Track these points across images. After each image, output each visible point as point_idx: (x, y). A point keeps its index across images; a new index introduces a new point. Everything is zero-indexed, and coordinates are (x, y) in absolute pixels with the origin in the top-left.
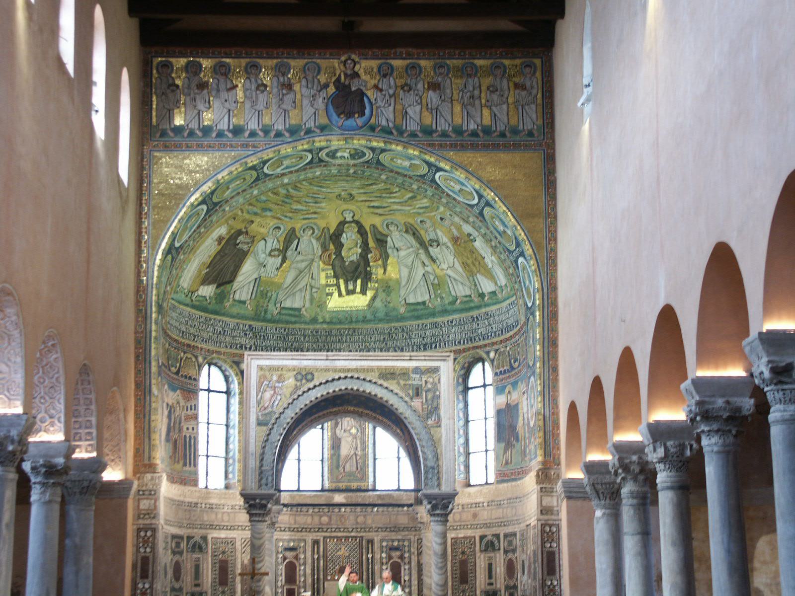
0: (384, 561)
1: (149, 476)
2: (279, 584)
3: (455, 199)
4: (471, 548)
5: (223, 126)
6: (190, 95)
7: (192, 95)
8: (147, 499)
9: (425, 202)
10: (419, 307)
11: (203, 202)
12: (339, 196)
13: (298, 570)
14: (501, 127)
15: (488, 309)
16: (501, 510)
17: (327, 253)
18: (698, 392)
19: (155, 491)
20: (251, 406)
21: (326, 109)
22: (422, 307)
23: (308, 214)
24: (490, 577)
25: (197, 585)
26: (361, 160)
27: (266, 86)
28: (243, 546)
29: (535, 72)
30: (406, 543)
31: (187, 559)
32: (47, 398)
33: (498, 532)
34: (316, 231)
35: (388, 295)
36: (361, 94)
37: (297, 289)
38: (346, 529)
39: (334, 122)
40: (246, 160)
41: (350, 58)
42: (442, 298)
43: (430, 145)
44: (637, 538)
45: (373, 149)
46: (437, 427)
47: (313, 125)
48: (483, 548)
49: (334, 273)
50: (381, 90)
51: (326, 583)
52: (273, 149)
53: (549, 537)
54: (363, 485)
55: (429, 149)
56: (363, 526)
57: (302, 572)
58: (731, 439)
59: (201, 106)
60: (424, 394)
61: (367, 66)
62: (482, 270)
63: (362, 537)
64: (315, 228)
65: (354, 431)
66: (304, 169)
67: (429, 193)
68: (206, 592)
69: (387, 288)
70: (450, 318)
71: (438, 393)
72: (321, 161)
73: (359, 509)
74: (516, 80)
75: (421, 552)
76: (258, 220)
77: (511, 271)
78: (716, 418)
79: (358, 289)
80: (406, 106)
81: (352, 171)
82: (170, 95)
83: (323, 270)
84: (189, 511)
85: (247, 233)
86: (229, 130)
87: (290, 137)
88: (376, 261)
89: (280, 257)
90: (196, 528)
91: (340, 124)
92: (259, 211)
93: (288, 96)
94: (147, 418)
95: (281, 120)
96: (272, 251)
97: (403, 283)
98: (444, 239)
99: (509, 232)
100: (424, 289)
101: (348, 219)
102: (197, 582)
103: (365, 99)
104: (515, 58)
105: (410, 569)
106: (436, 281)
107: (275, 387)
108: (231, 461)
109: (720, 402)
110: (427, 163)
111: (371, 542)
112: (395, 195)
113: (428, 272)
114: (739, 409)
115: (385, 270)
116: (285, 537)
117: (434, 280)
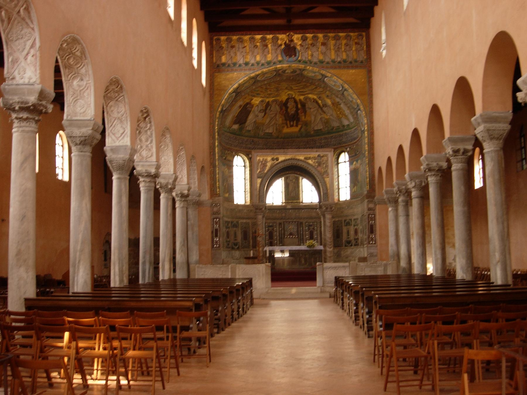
0: (307, 230)
1: (217, 198)
2: (267, 240)
5: (241, 62)
6: (227, 50)
9: (321, 90)
12: (286, 88)
14: (350, 60)
15: (347, 131)
18: (427, 160)
24: (348, 235)
25: (236, 240)
26: (296, 74)
29: (363, 39)
30: (315, 223)
32: (180, 168)
33: (350, 218)
36: (294, 48)
43: (323, 67)
44: (405, 217)
45: (300, 70)
48: (345, 224)
50: (303, 46)
51: (285, 240)
53: (371, 219)
54: (298, 201)
58: (438, 178)
59: (232, 54)
61: (297, 38)
62: (344, 116)
63: (298, 222)
65: (294, 180)
66: (272, 78)
69: (306, 124)
70: (332, 135)
72: (279, 74)
73: (297, 211)
74: (356, 41)
76: (255, 99)
77: (355, 116)
78: (434, 170)
79: (295, 125)
81: (291, 78)
83: (281, 117)
87: (267, 65)
88: (302, 113)
89: (263, 114)
91: (287, 60)
92: (255, 95)
96: (260, 110)
97: (313, 122)
101: (290, 97)
103: (297, 50)
104: (355, 32)
108: (246, 193)
109: (435, 164)
111: (302, 223)
114: (441, 167)
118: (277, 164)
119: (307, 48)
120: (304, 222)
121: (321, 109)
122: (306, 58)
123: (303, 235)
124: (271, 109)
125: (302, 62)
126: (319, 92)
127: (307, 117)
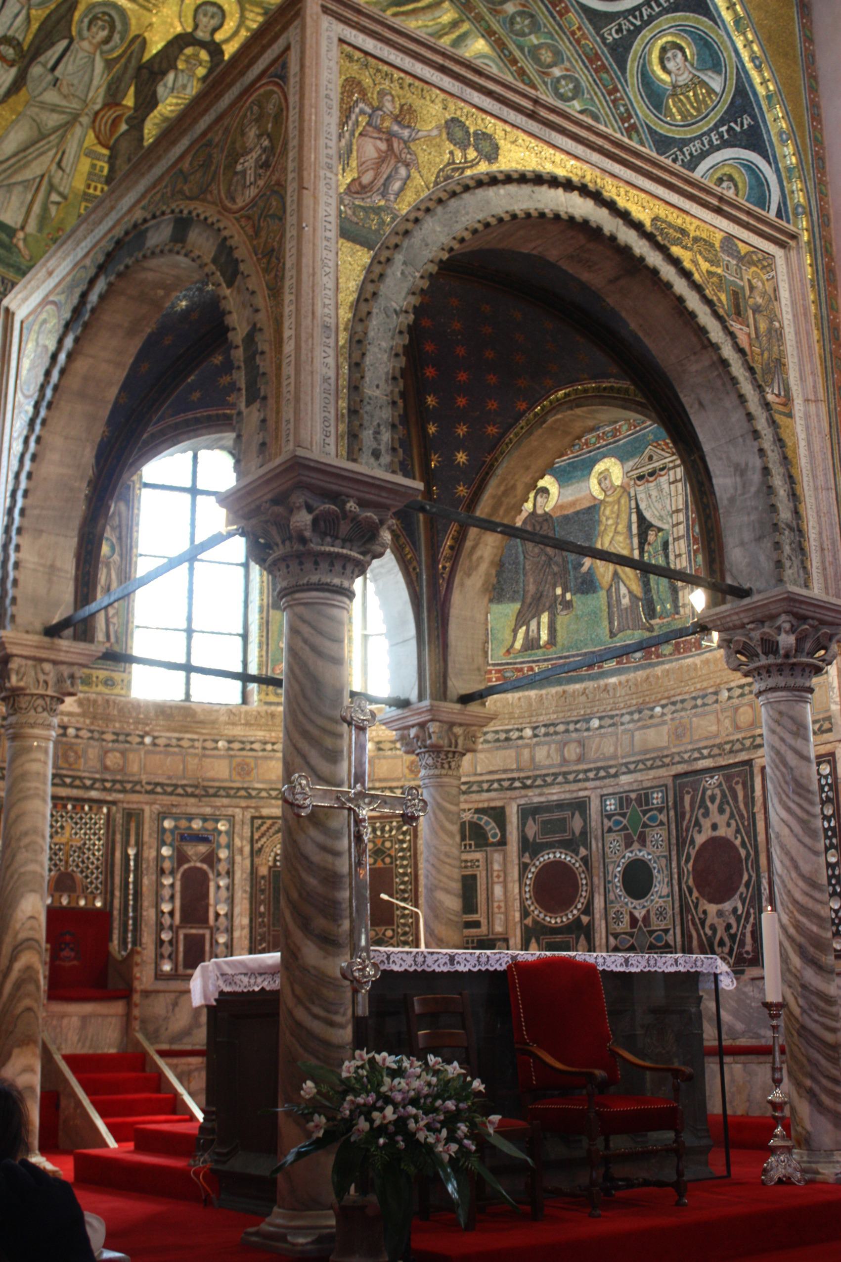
4: (402, 841)
16: (512, 753)
17: (112, 114)
20: (323, 160)
33: (498, 804)
34: (116, 37)
37: (19, 178)
49: (112, 170)
56: (119, 777)
60: (750, 312)
63: (114, 803)
64: (119, 26)
75: (260, 850)
83: (90, 154)
89: (13, 71)
99: (716, 83)
101: (200, 34)
105: (230, 888)
111: (133, 816)
118: (493, 181)
120: (148, 812)
123: (137, 894)
124: (58, 73)
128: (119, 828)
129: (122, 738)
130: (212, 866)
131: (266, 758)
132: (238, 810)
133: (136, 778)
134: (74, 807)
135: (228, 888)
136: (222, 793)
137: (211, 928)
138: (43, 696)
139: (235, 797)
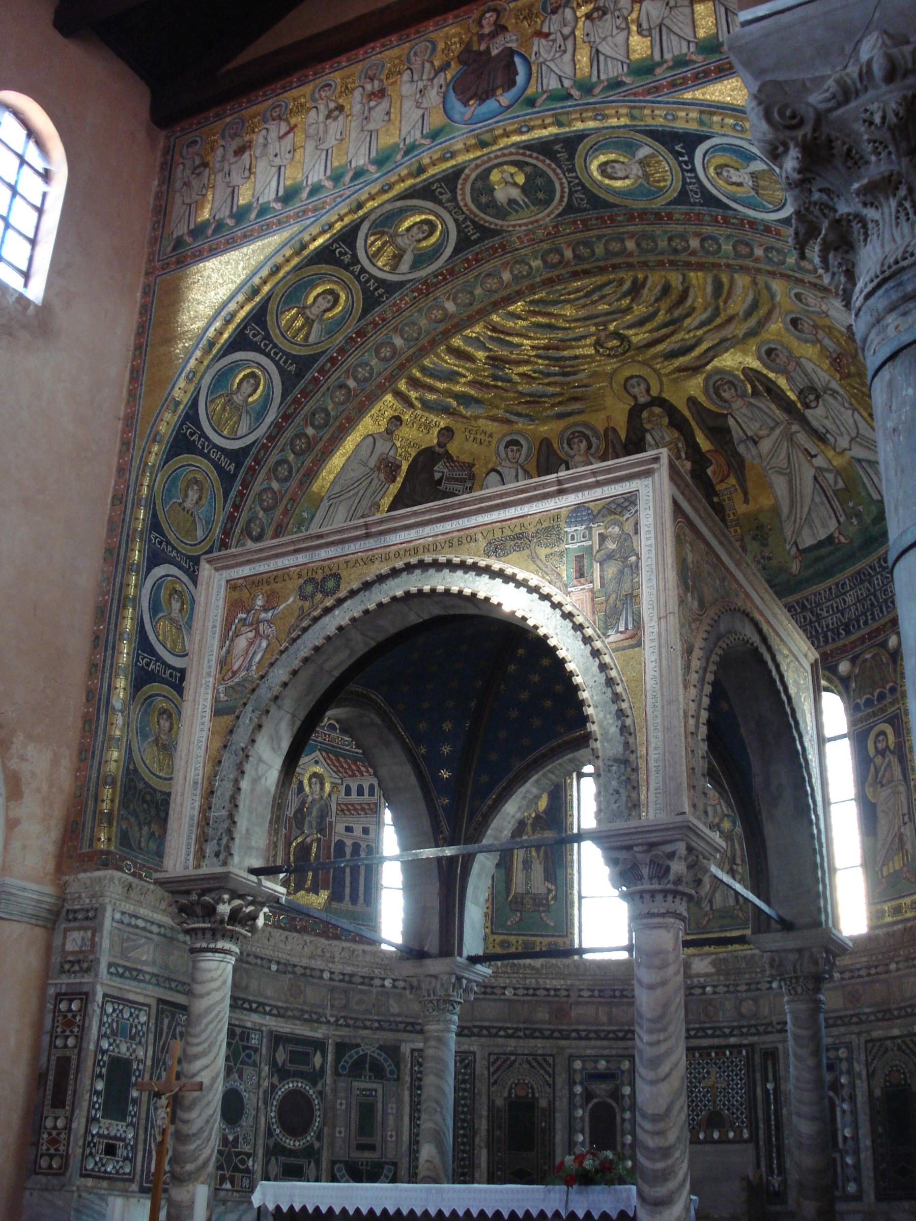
3: (767, 229)
7: (226, 169)
8: (79, 929)
10: (823, 551)
11: (239, 342)
13: (618, 1120)
19: (96, 909)
20: (205, 670)
21: (444, 103)
22: (831, 548)
23: (560, 403)
27: (340, 108)
28: (492, 1070)
30: (843, 1053)
31: (335, 1091)
34: (594, 440)
35: (765, 545)
38: (718, 1031)
39: (457, 117)
40: (300, 236)
41: (488, 11)
42: (858, 515)
43: (649, 92)
45: (544, 148)
46: (632, 647)
47: (418, 135)
52: (348, 201)
55: (648, 98)
56: (753, 1022)
57: (627, 1126)
59: (236, 179)
63: (752, 1045)
67: (727, 247)
68: (395, 1164)
71: (633, 559)
72: (486, 232)
75: (874, 1071)
76: (458, 426)
80: (598, 40)
81: (568, 254)
82: (194, 182)
84: (345, 992)
85: (449, 457)
86: (278, 199)
87: (377, 172)
90: (365, 1028)
91: (467, 117)
93: (377, 109)
94: (97, 758)
95: (364, 150)
97: (785, 510)
98: (823, 375)
100: (824, 510)
101: (642, 400)
102: (365, 1140)
103: (517, 60)
105: (854, 1112)
106: (841, 485)
107: (258, 622)
110: (654, 134)
112: (689, 302)
113: (819, 469)
115: (745, 493)
116: (589, 1052)
117: (836, 482)
119: (565, 38)
121: (804, 422)
122: (560, 77)
125: (540, 101)
126: (748, 314)
127: (752, 492)
128: (758, 1068)
129: (753, 987)
130: (836, 1092)
131: (872, 982)
132: (854, 1036)
133: (767, 1021)
134: (717, 1054)
135: (851, 1112)
136: (839, 1022)
137: (840, 1151)
138: (431, 1002)
139: (850, 1024)
